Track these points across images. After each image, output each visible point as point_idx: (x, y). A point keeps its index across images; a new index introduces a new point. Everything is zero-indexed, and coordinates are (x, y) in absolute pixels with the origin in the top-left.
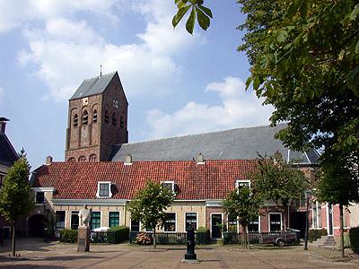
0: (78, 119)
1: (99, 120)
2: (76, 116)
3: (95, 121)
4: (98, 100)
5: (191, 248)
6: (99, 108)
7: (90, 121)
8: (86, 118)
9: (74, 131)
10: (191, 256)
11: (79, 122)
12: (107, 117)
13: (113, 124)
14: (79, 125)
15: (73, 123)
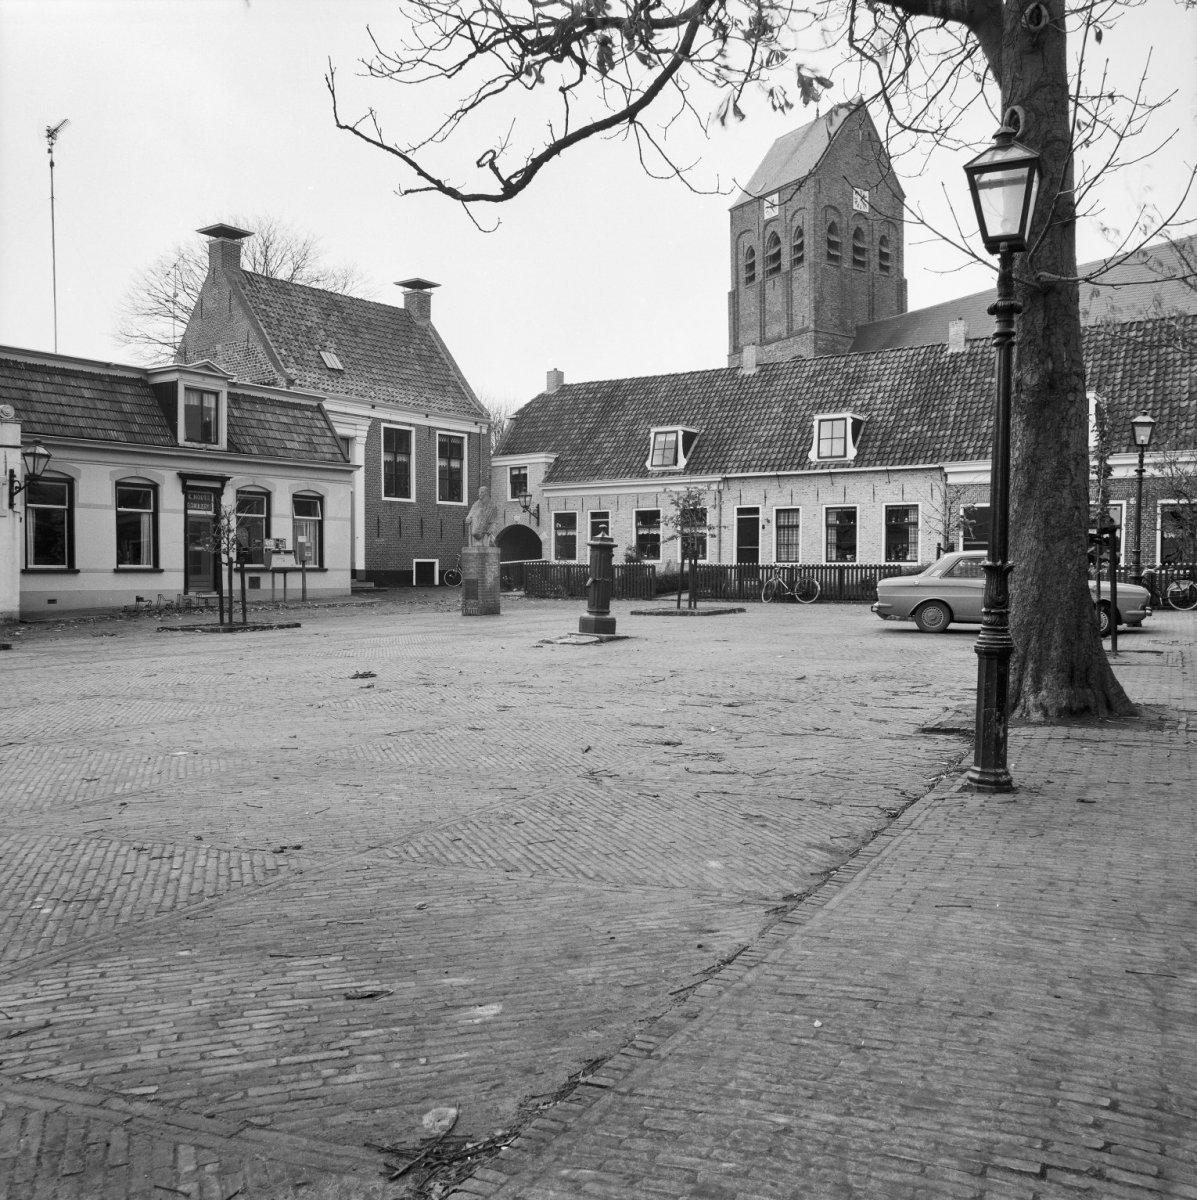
2: (751, 253)
3: (800, 260)
4: (806, 199)
5: (601, 606)
6: (806, 219)
7: (785, 262)
8: (777, 256)
10: (602, 628)
11: (759, 269)
12: (832, 244)
13: (856, 262)
14: (759, 278)
15: (743, 275)
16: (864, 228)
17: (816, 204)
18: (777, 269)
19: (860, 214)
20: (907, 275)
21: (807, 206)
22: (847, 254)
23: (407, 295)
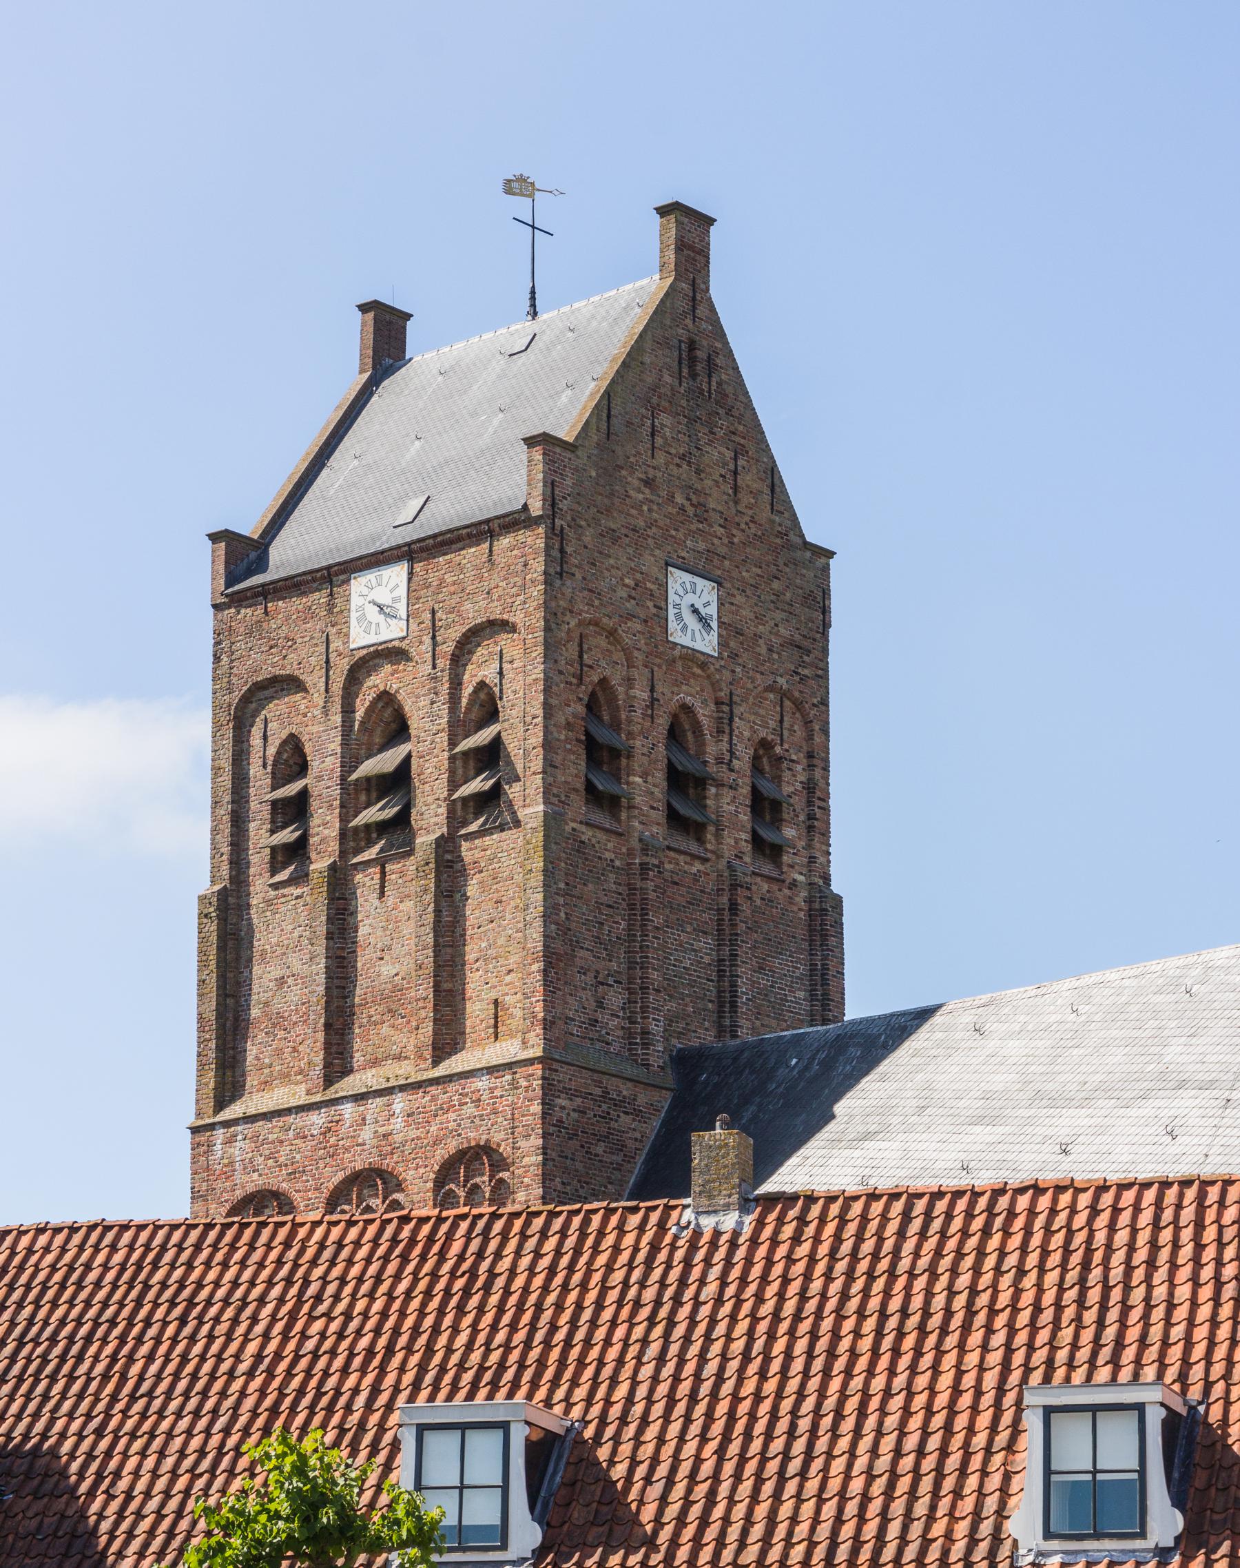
0: (310, 805)
2: (293, 760)
4: (512, 584)
6: (518, 674)
8: (398, 782)
9: (287, 930)
11: (325, 826)
13: (675, 819)
14: (319, 864)
16: (705, 714)
18: (402, 821)
19: (692, 657)
20: (843, 878)
21: (517, 618)
22: (645, 787)
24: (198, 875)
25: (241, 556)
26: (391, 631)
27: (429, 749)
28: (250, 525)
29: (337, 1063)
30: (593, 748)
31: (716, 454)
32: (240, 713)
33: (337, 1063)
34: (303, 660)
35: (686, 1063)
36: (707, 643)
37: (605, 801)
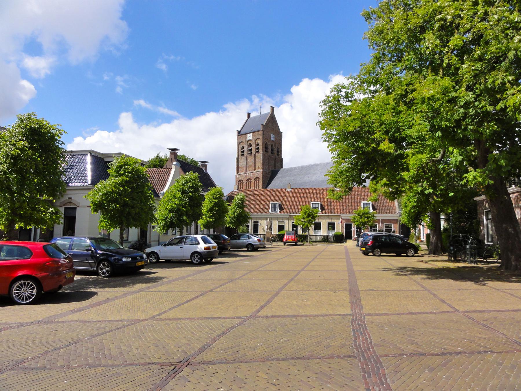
1: (261, 150)
2: (243, 148)
4: (260, 135)
7: (254, 152)
8: (251, 150)
9: (243, 161)
11: (245, 153)
14: (245, 155)
15: (241, 153)
17: (263, 137)
18: (251, 153)
19: (273, 141)
22: (269, 150)
23: (170, 152)
24: (236, 156)
25: (239, 132)
26: (251, 138)
27: (254, 147)
28: (239, 130)
29: (246, 171)
30: (266, 148)
31: (275, 125)
32: (239, 144)
33: (246, 171)
34: (244, 141)
35: (272, 171)
36: (274, 140)
37: (266, 151)
